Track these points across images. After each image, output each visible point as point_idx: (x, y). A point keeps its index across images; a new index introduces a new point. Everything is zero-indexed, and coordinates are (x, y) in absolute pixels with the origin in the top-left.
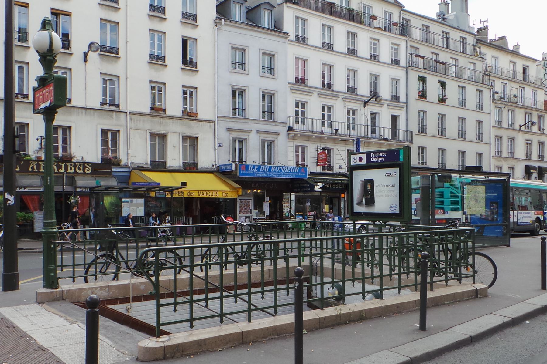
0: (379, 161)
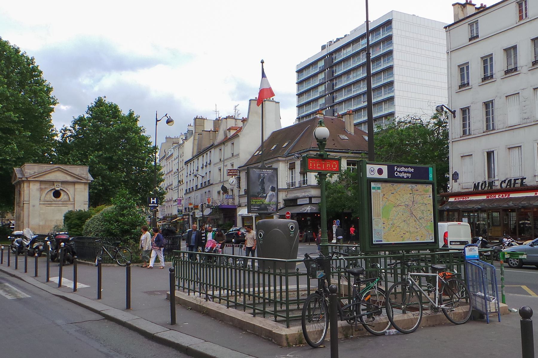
0: (405, 177)
